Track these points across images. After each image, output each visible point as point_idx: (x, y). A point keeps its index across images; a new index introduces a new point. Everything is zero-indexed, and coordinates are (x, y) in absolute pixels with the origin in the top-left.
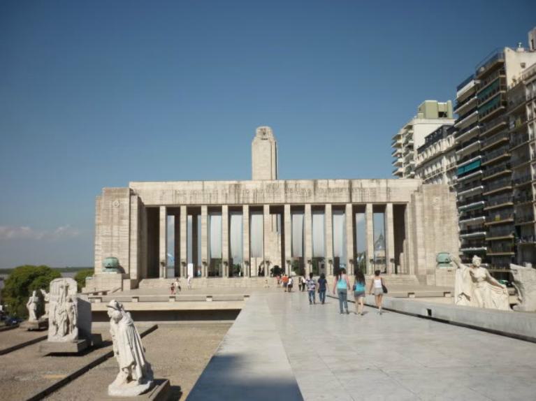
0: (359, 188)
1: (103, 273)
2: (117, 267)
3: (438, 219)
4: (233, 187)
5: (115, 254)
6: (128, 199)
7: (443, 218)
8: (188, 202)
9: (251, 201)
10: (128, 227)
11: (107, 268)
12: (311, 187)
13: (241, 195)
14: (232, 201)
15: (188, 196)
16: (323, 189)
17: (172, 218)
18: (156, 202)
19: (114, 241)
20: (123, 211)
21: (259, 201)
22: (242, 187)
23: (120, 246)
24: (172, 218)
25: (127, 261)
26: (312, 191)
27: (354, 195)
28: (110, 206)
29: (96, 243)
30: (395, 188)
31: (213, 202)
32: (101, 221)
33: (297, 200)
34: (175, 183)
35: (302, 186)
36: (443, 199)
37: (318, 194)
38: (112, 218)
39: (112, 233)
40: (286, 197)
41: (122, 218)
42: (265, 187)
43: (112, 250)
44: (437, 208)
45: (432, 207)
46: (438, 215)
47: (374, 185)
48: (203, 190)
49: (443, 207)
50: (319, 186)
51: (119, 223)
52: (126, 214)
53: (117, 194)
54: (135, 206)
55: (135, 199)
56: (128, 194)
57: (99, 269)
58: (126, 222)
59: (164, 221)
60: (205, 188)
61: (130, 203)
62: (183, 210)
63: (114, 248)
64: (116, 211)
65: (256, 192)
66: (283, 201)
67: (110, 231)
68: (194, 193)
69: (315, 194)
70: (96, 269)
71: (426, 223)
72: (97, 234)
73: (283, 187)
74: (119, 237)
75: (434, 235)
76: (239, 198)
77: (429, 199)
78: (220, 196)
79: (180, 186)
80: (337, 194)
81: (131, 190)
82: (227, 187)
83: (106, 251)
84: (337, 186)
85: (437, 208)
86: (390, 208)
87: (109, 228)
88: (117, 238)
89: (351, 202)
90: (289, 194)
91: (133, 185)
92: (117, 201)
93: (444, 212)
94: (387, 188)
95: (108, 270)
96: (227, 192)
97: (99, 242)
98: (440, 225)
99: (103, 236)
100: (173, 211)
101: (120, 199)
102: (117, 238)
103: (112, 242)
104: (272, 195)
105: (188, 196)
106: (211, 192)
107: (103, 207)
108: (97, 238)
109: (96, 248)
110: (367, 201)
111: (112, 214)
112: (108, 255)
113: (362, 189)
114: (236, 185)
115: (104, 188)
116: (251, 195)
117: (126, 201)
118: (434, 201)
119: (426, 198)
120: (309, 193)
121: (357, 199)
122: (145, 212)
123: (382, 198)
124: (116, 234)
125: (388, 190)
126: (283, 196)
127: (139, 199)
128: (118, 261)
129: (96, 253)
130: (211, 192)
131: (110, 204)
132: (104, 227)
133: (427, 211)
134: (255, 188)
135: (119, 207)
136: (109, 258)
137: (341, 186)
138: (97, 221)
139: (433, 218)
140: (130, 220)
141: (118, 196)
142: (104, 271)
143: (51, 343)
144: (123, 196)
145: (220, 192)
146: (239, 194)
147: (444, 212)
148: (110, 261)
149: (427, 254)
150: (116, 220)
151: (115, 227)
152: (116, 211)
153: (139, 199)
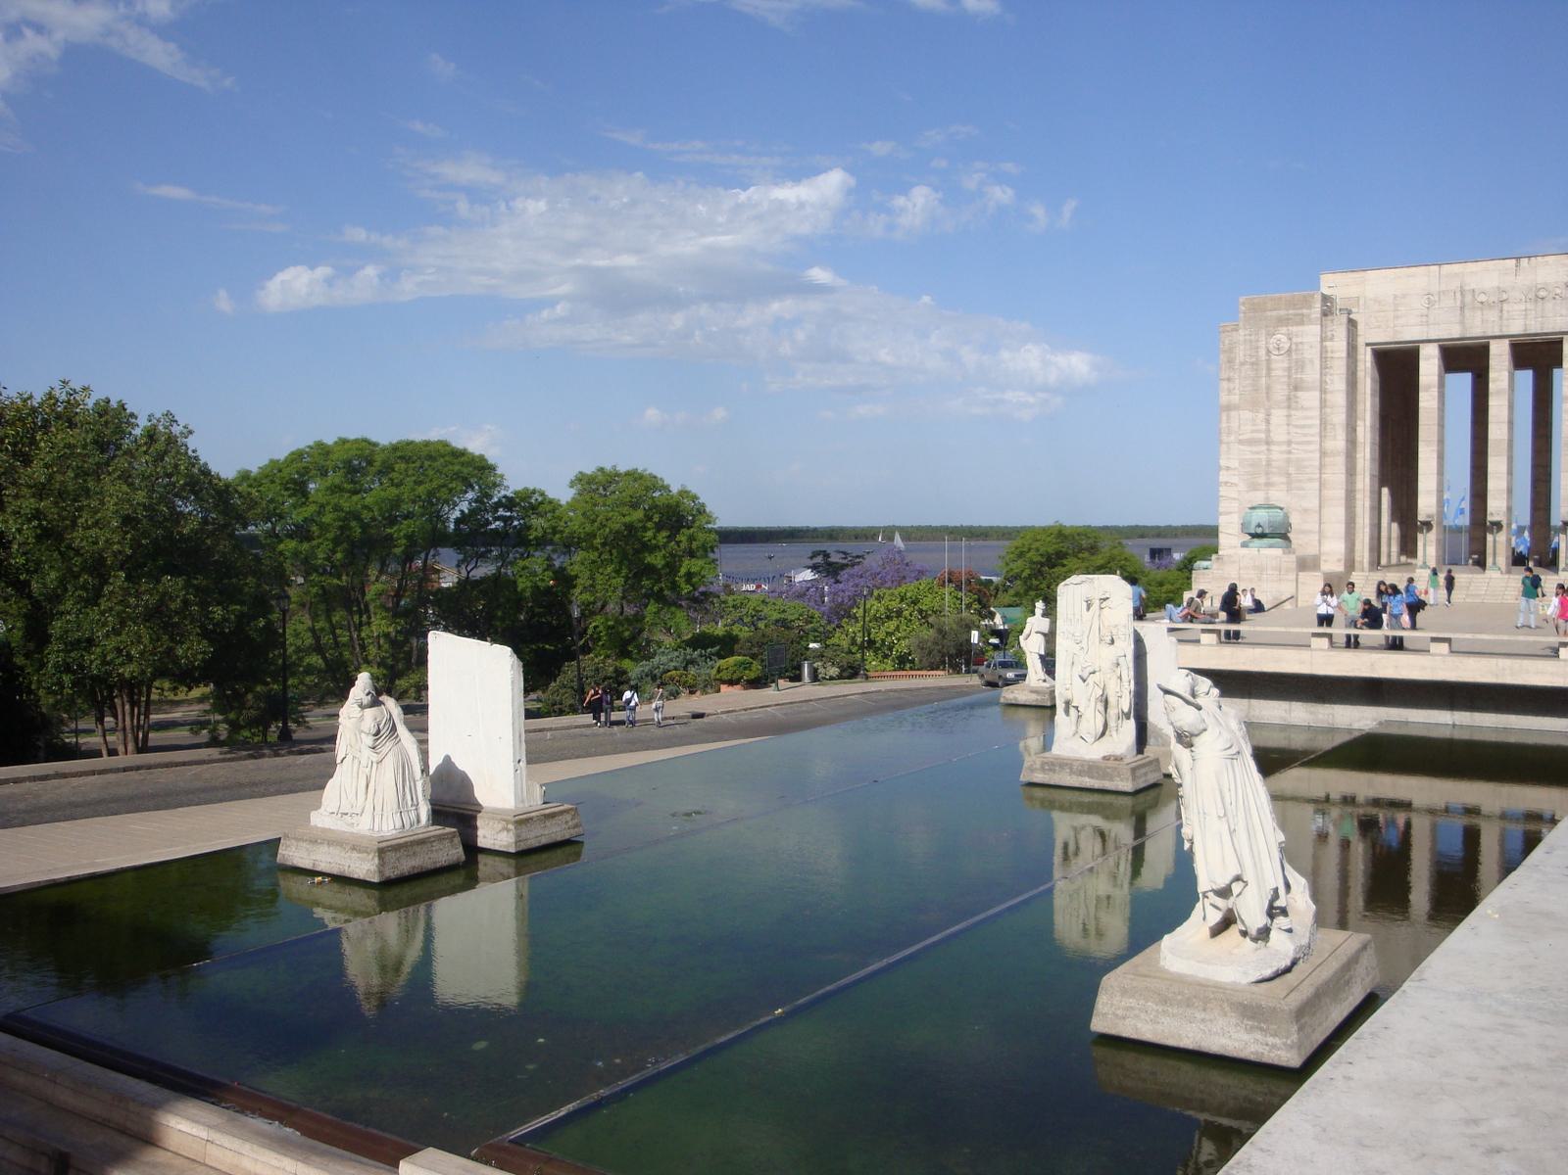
1: (1245, 551)
2: (1278, 533)
5: (1278, 496)
8: (1516, 327)
10: (1316, 413)
11: (1255, 536)
17: (1463, 381)
19: (1275, 456)
20: (1301, 365)
23: (1292, 470)
28: (1262, 352)
29: (1223, 463)
32: (1235, 399)
34: (1471, 267)
38: (1268, 388)
39: (1268, 431)
43: (1268, 484)
51: (1290, 403)
52: (1312, 374)
53: (1282, 313)
54: (1339, 346)
57: (1230, 539)
58: (1310, 399)
59: (1435, 392)
61: (1323, 340)
62: (1500, 357)
63: (1275, 479)
64: (1280, 364)
68: (1537, 297)
70: (1224, 540)
72: (1224, 438)
74: (1289, 443)
79: (1486, 276)
81: (1325, 298)
83: (1254, 487)
87: (1261, 416)
88: (1284, 448)
91: (1334, 284)
92: (1281, 336)
95: (1257, 541)
97: (1232, 458)
99: (1241, 442)
101: (1294, 329)
102: (1284, 448)
103: (1269, 464)
107: (1241, 353)
108: (1224, 447)
109: (1223, 476)
111: (1268, 375)
112: (1259, 497)
115: (1242, 299)
117: (1310, 333)
124: (1279, 434)
127: (1352, 324)
128: (1286, 516)
129: (1223, 491)
131: (1262, 344)
132: (1246, 415)
135: (1289, 351)
136: (1260, 507)
138: (1224, 399)
140: (1323, 391)
141: (1283, 321)
142: (1244, 545)
143: (1057, 758)
148: (1261, 516)
150: (1280, 392)
151: (1278, 416)
152: (1280, 364)
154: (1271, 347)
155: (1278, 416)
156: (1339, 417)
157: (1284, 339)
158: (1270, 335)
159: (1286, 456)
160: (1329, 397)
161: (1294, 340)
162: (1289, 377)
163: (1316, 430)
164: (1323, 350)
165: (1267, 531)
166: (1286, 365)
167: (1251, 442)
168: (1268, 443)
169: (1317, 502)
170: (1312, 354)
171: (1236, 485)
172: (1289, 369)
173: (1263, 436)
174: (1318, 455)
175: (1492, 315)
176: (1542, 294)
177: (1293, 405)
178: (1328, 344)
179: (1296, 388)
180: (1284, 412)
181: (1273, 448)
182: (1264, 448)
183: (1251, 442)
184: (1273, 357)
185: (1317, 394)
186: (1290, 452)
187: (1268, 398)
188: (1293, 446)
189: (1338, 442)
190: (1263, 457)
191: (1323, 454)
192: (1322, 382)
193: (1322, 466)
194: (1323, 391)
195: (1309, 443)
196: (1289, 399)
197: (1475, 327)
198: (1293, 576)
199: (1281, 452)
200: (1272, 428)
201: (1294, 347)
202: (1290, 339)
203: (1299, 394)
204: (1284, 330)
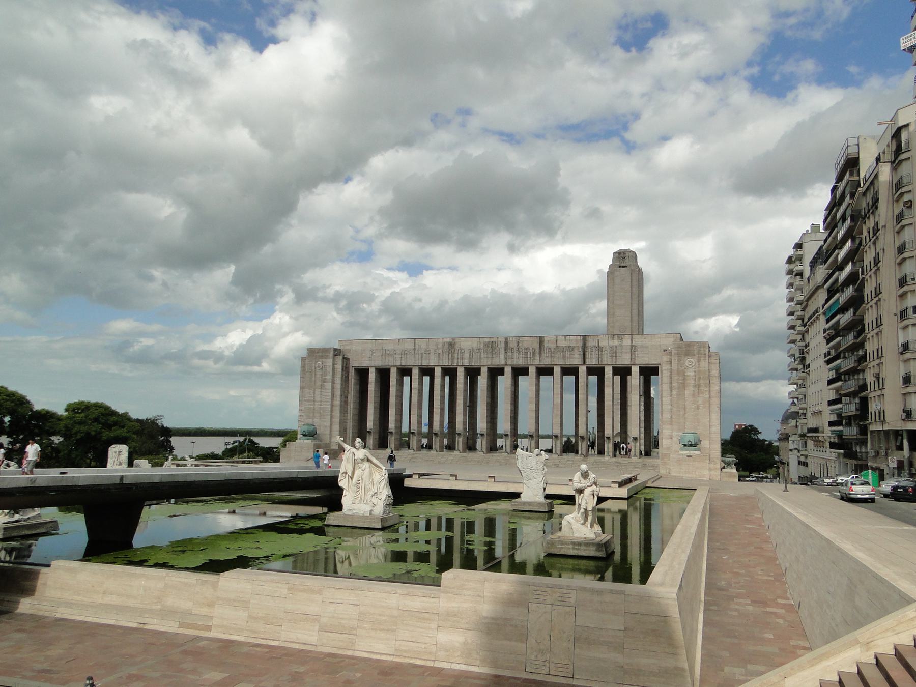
3: (692, 388)
4: (447, 345)
5: (317, 422)
7: (698, 386)
9: (466, 363)
12: (536, 345)
13: (456, 355)
14: (446, 363)
15: (398, 356)
16: (550, 349)
18: (364, 363)
20: (325, 374)
21: (475, 363)
22: (457, 346)
24: (426, 379)
25: (329, 429)
26: (538, 351)
27: (588, 355)
30: (642, 346)
31: (425, 363)
33: (520, 362)
35: (525, 345)
36: (699, 361)
37: (544, 355)
40: (506, 358)
41: (324, 381)
42: (482, 346)
43: (314, 417)
46: (691, 382)
47: (616, 342)
48: (415, 349)
49: (699, 371)
50: (546, 345)
51: (322, 387)
52: (329, 377)
54: (339, 367)
55: (339, 360)
56: (331, 355)
58: (328, 385)
60: (417, 347)
61: (334, 364)
64: (319, 373)
65: (472, 351)
66: (503, 363)
68: (404, 353)
69: (540, 354)
71: (674, 393)
73: (503, 345)
75: (685, 409)
76: (453, 359)
77: (679, 361)
78: (432, 357)
80: (567, 354)
82: (440, 346)
83: (309, 417)
84: (568, 344)
85: (690, 373)
90: (509, 354)
93: (700, 378)
94: (632, 346)
96: (440, 351)
98: (694, 395)
100: (405, 371)
104: (490, 355)
105: (398, 356)
106: (423, 352)
112: (310, 421)
113: (600, 349)
114: (450, 344)
116: (467, 355)
117: (329, 362)
118: (687, 364)
119: (675, 360)
120: (534, 354)
121: (592, 361)
122: (352, 372)
124: (318, 398)
125: (633, 348)
126: (502, 356)
130: (423, 352)
132: (307, 390)
133: (675, 377)
134: (470, 347)
137: (572, 344)
139: (683, 386)
140: (333, 382)
141: (322, 357)
145: (432, 352)
146: (453, 353)
147: (700, 378)
150: (319, 383)
151: (318, 391)
152: (319, 373)
155: (318, 391)
156: (338, 392)
167: (308, 401)
170: (330, 370)
175: (391, 359)
183: (308, 401)
189: (337, 402)
191: (332, 406)
194: (333, 382)
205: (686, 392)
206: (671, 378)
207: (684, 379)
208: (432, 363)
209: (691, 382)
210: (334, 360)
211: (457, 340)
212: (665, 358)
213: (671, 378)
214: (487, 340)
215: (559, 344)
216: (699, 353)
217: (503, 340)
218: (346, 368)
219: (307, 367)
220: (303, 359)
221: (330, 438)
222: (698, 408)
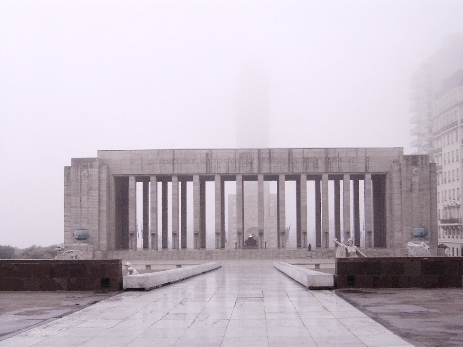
0: (335, 157)
1: (74, 244)
5: (84, 225)
6: (97, 170)
8: (158, 172)
10: (97, 197)
13: (213, 165)
23: (89, 217)
31: (183, 172)
42: (237, 157)
43: (81, 222)
44: (416, 179)
45: (411, 180)
48: (174, 160)
52: (96, 185)
54: (104, 176)
56: (97, 164)
58: (95, 193)
61: (100, 173)
64: (85, 181)
67: (79, 202)
68: (163, 162)
71: (404, 195)
73: (256, 156)
74: (88, 207)
86: (368, 177)
87: (79, 198)
89: (326, 172)
101: (90, 169)
102: (86, 209)
110: (344, 171)
112: (78, 226)
113: (340, 160)
117: (95, 171)
123: (360, 169)
127: (108, 168)
131: (79, 174)
132: (73, 198)
133: (404, 183)
135: (88, 177)
137: (317, 156)
140: (99, 190)
144: (91, 167)
148: (81, 232)
149: (404, 228)
151: (84, 198)
153: (108, 168)
154: (82, 175)
157: (86, 173)
158: (81, 171)
159: (87, 212)
160: (101, 192)
161: (90, 173)
162: (88, 185)
163: (97, 203)
164: (99, 177)
165: (82, 238)
166: (87, 181)
167: (74, 207)
168: (81, 207)
169: (97, 228)
170: (95, 178)
171: (70, 222)
172: (88, 183)
173: (79, 205)
174: (97, 212)
176: (165, 162)
177: (89, 195)
178: (100, 175)
179: (90, 189)
180: (87, 197)
181: (82, 209)
182: (80, 209)
183: (74, 207)
184: (82, 179)
185: (97, 191)
186: (88, 211)
187: (81, 193)
188: (90, 208)
189: (104, 208)
190: (79, 212)
191: (99, 211)
192: (99, 188)
193: (99, 215)
195: (95, 208)
196: (88, 193)
197: (146, 171)
198: (91, 253)
199: (85, 211)
200: (82, 202)
201: (89, 175)
202: (89, 173)
203: (91, 191)
204: (86, 170)
205: (413, 195)
206: (401, 184)
207: (412, 185)
208: (190, 172)
209: (416, 186)
210: (99, 169)
211: (214, 151)
212: (396, 168)
213: (401, 184)
214: (240, 151)
215: (306, 155)
216: (422, 164)
217: (257, 151)
218: (108, 177)
219: (72, 176)
220: (67, 169)
221: (99, 241)
222: (422, 207)
